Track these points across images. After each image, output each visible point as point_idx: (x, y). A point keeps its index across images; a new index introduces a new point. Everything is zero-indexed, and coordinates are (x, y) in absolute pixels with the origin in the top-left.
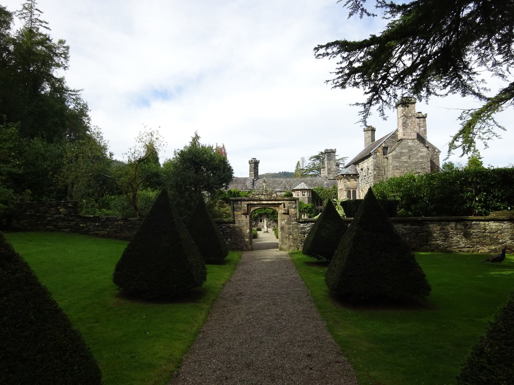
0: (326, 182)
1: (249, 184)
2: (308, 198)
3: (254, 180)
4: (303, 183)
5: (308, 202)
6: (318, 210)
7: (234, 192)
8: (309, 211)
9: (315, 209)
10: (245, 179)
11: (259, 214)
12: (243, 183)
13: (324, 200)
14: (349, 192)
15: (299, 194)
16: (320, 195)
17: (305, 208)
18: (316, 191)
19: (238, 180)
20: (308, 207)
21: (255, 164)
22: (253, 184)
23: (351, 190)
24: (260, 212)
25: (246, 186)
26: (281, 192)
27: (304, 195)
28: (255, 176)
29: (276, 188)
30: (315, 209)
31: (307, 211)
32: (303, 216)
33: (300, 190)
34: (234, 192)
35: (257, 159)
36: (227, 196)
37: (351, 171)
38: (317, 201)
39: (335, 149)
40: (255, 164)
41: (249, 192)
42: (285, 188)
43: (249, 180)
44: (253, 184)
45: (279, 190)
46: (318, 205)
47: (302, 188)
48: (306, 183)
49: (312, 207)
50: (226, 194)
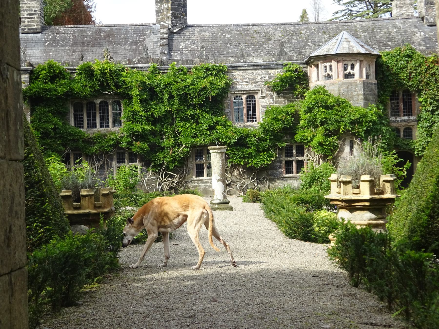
0: (420, 35)
1: (154, 45)
2: (366, 85)
3: (171, 33)
4: (345, 35)
5: (366, 99)
6: (397, 130)
7: (103, 73)
8: (368, 132)
9: (388, 125)
10: (141, 30)
11: (193, 147)
12: (135, 43)
13: (419, 92)
15: (334, 74)
16: (403, 75)
17: (353, 123)
18: (391, 62)
20: (364, 116)
22: (170, 45)
24: (197, 141)
25: (146, 50)
26: (268, 67)
27: (347, 76)
28: (175, 17)
29: (249, 55)
30: (388, 125)
31: (361, 130)
32: (347, 149)
33: (337, 57)
34: (103, 73)
36: (77, 87)
38: (394, 96)
41: (155, 71)
42: (282, 53)
43: (157, 32)
44: (170, 45)
45: (259, 61)
46: (396, 113)
47: (344, 49)
48: (355, 34)
49: (380, 117)
50: (72, 80)
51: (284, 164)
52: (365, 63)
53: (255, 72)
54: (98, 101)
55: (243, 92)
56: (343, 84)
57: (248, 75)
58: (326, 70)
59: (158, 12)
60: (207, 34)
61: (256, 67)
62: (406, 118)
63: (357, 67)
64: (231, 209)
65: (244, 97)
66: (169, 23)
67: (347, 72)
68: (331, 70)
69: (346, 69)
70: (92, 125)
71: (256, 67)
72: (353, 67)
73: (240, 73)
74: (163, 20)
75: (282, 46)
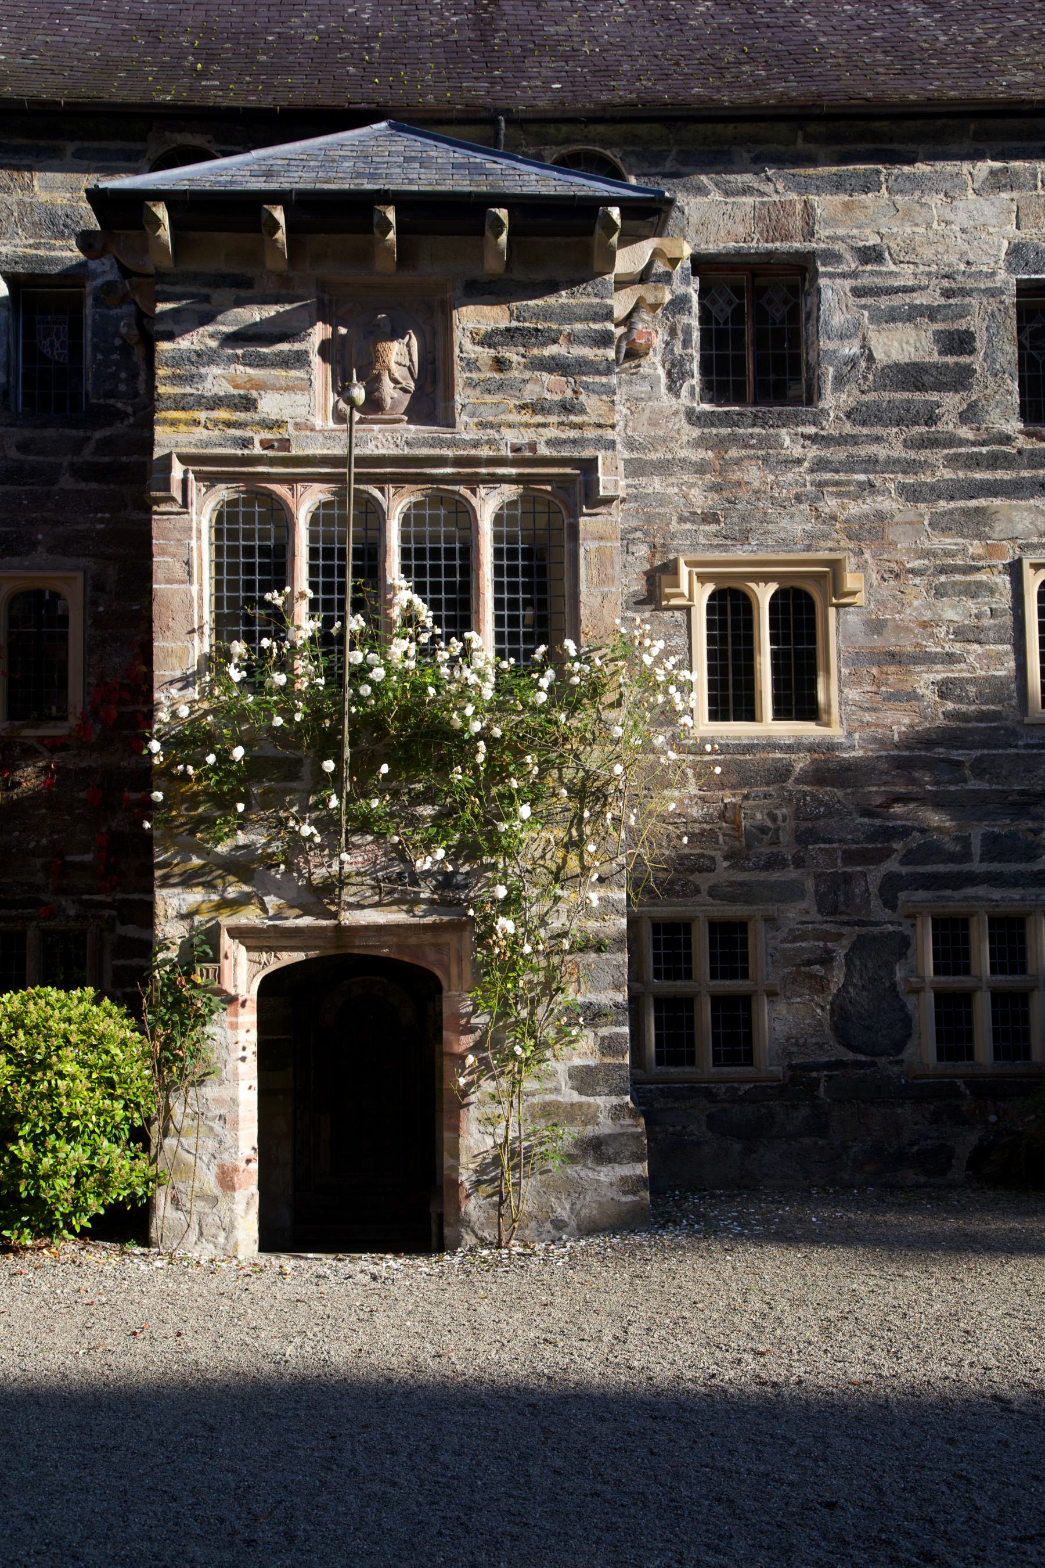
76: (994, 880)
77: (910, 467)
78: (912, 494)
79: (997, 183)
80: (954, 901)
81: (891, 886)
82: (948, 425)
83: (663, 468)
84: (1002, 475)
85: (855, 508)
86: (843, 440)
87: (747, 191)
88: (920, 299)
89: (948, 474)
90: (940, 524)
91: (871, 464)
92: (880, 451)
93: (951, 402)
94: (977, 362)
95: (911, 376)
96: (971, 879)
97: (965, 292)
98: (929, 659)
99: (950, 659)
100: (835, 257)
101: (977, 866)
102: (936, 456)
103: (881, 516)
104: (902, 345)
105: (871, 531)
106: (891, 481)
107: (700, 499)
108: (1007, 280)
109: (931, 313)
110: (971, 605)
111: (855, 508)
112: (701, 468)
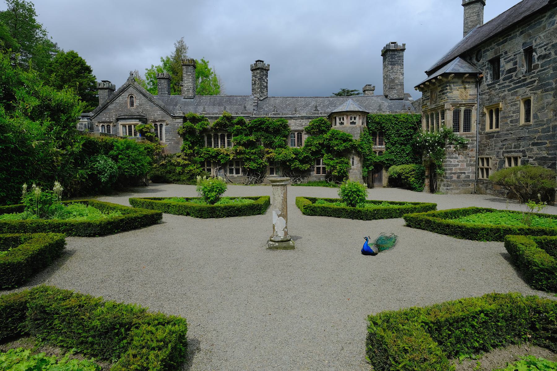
10: (244, 98)
14: (456, 114)
19: (230, 99)
21: (260, 70)
23: (463, 109)
27: (352, 123)
35: (266, 63)
37: (462, 67)
39: (404, 45)
40: (260, 70)
45: (304, 115)
51: (315, 169)
52: (361, 116)
53: (302, 120)
54: (219, 134)
55: (296, 131)
56: (350, 127)
57: (298, 122)
58: (340, 120)
59: (253, 90)
60: (277, 101)
61: (302, 118)
62: (380, 146)
63: (357, 118)
64: (293, 248)
65: (296, 133)
66: (258, 95)
67: (351, 121)
68: (343, 120)
69: (351, 119)
70: (216, 145)
71: (302, 118)
72: (355, 118)
73: (294, 121)
74: (255, 93)
75: (316, 107)
76: (515, 152)
77: (509, 86)
78: (509, 91)
79: (522, 33)
80: (510, 155)
81: (504, 152)
82: (514, 78)
83: (484, 94)
84: (520, 84)
85: (503, 94)
86: (503, 84)
87: (494, 48)
88: (511, 58)
89: (513, 86)
90: (512, 95)
91: (504, 87)
92: (506, 85)
93: (514, 74)
94: (517, 66)
95: (510, 71)
96: (511, 152)
97: (516, 54)
98: (509, 117)
99: (512, 116)
100: (502, 55)
101: (513, 150)
102: (511, 84)
103: (505, 95)
104: (509, 66)
105: (504, 98)
106: (506, 89)
107: (488, 97)
108: (522, 50)
109: (512, 60)
110: (515, 107)
111: (503, 94)
112: (488, 93)
